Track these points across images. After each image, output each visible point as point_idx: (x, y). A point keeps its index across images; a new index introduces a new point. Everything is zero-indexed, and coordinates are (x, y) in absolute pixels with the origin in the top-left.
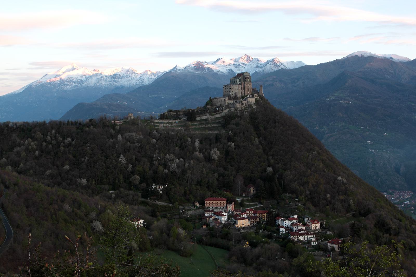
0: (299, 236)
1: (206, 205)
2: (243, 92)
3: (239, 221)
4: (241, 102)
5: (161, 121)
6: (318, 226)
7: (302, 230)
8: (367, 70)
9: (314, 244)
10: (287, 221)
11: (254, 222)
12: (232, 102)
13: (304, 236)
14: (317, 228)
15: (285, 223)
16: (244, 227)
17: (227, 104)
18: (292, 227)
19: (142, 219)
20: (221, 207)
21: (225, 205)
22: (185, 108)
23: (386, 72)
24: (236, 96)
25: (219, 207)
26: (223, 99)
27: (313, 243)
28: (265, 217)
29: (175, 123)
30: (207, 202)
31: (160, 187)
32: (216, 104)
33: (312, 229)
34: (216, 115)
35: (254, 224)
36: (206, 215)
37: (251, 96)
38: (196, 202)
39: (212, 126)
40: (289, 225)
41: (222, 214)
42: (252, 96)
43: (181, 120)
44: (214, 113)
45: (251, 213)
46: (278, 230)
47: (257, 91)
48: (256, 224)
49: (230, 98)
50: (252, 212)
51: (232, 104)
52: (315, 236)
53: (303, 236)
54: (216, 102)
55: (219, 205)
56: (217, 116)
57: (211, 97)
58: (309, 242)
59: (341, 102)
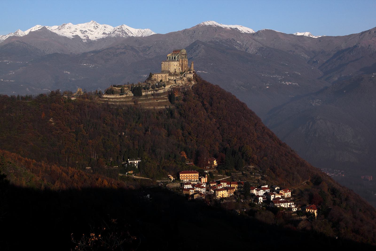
0: (280, 204)
1: (180, 178)
2: (181, 69)
3: (219, 192)
5: (109, 96)
6: (290, 194)
8: (216, 40)
10: (261, 191)
11: (231, 192)
12: (172, 78)
14: (289, 196)
15: (260, 193)
17: (168, 80)
19: (149, 194)
20: (195, 180)
23: (235, 43)
24: (175, 71)
25: (193, 180)
26: (164, 75)
27: (294, 209)
29: (122, 98)
30: (181, 175)
31: (136, 162)
32: (155, 79)
33: (286, 197)
34: (160, 91)
35: (231, 195)
37: (188, 72)
38: (169, 175)
39: (158, 101)
41: (202, 186)
42: (189, 73)
43: (127, 95)
44: (157, 89)
45: (225, 184)
48: (233, 194)
49: (170, 74)
50: (226, 183)
51: (172, 80)
53: (284, 204)
54: (157, 78)
56: (161, 91)
57: (151, 72)
58: (290, 209)
59: (198, 72)
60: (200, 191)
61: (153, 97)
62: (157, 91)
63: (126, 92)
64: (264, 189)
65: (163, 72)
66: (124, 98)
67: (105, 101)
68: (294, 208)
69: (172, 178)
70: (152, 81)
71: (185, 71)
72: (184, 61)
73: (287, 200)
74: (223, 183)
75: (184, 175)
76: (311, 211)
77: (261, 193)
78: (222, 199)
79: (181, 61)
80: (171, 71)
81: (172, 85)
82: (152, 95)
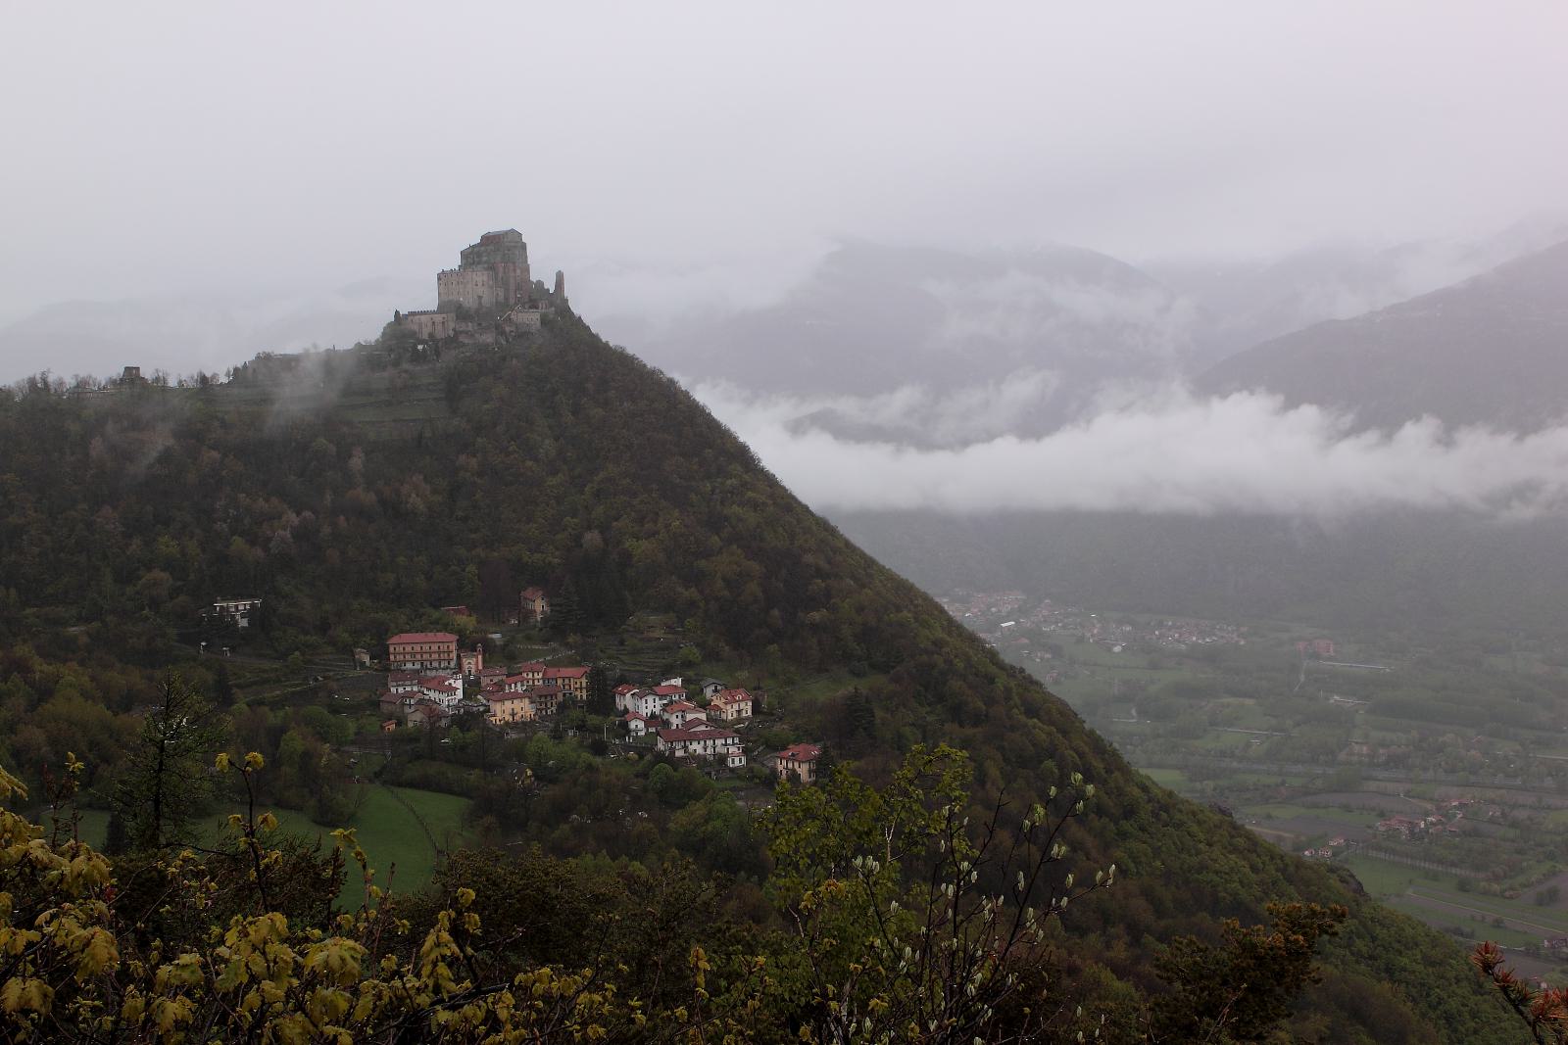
1: (392, 657)
2: (501, 294)
6: (747, 708)
7: (699, 722)
9: (737, 763)
10: (650, 699)
12: (470, 327)
13: (705, 742)
14: (744, 715)
16: (517, 723)
17: (451, 333)
18: (666, 716)
21: (454, 655)
22: (315, 346)
24: (480, 303)
26: (438, 318)
27: (733, 760)
32: (413, 334)
33: (730, 718)
36: (393, 690)
41: (446, 683)
47: (548, 290)
50: (541, 675)
52: (737, 741)
54: (415, 328)
58: (722, 759)
60: (437, 700)
72: (512, 268)
73: (719, 726)
75: (404, 649)
77: (651, 705)
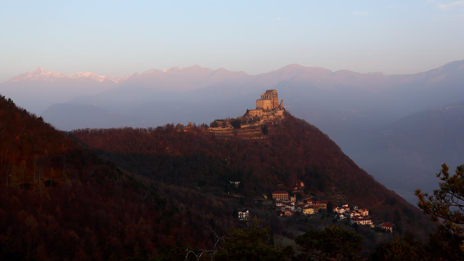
1: (273, 197)
2: (272, 106)
3: (306, 209)
4: (273, 114)
5: (213, 129)
6: (367, 212)
7: (359, 216)
10: (342, 209)
12: (265, 114)
14: (367, 215)
17: (262, 115)
21: (288, 197)
22: (229, 118)
25: (284, 199)
26: (258, 111)
28: (322, 206)
31: (236, 183)
37: (279, 109)
40: (344, 212)
46: (338, 217)
49: (264, 111)
50: (312, 202)
55: (284, 197)
56: (257, 124)
60: (289, 208)
61: (249, 129)
62: (252, 124)
63: (227, 125)
64: (345, 208)
65: (257, 109)
66: (226, 130)
67: (210, 133)
68: (372, 225)
69: (266, 197)
70: (249, 116)
71: (276, 108)
72: (275, 99)
73: (365, 218)
74: (309, 202)
76: (387, 228)
77: (342, 211)
78: (309, 215)
79: (272, 100)
80: (264, 108)
81: (265, 119)
82: (248, 128)
